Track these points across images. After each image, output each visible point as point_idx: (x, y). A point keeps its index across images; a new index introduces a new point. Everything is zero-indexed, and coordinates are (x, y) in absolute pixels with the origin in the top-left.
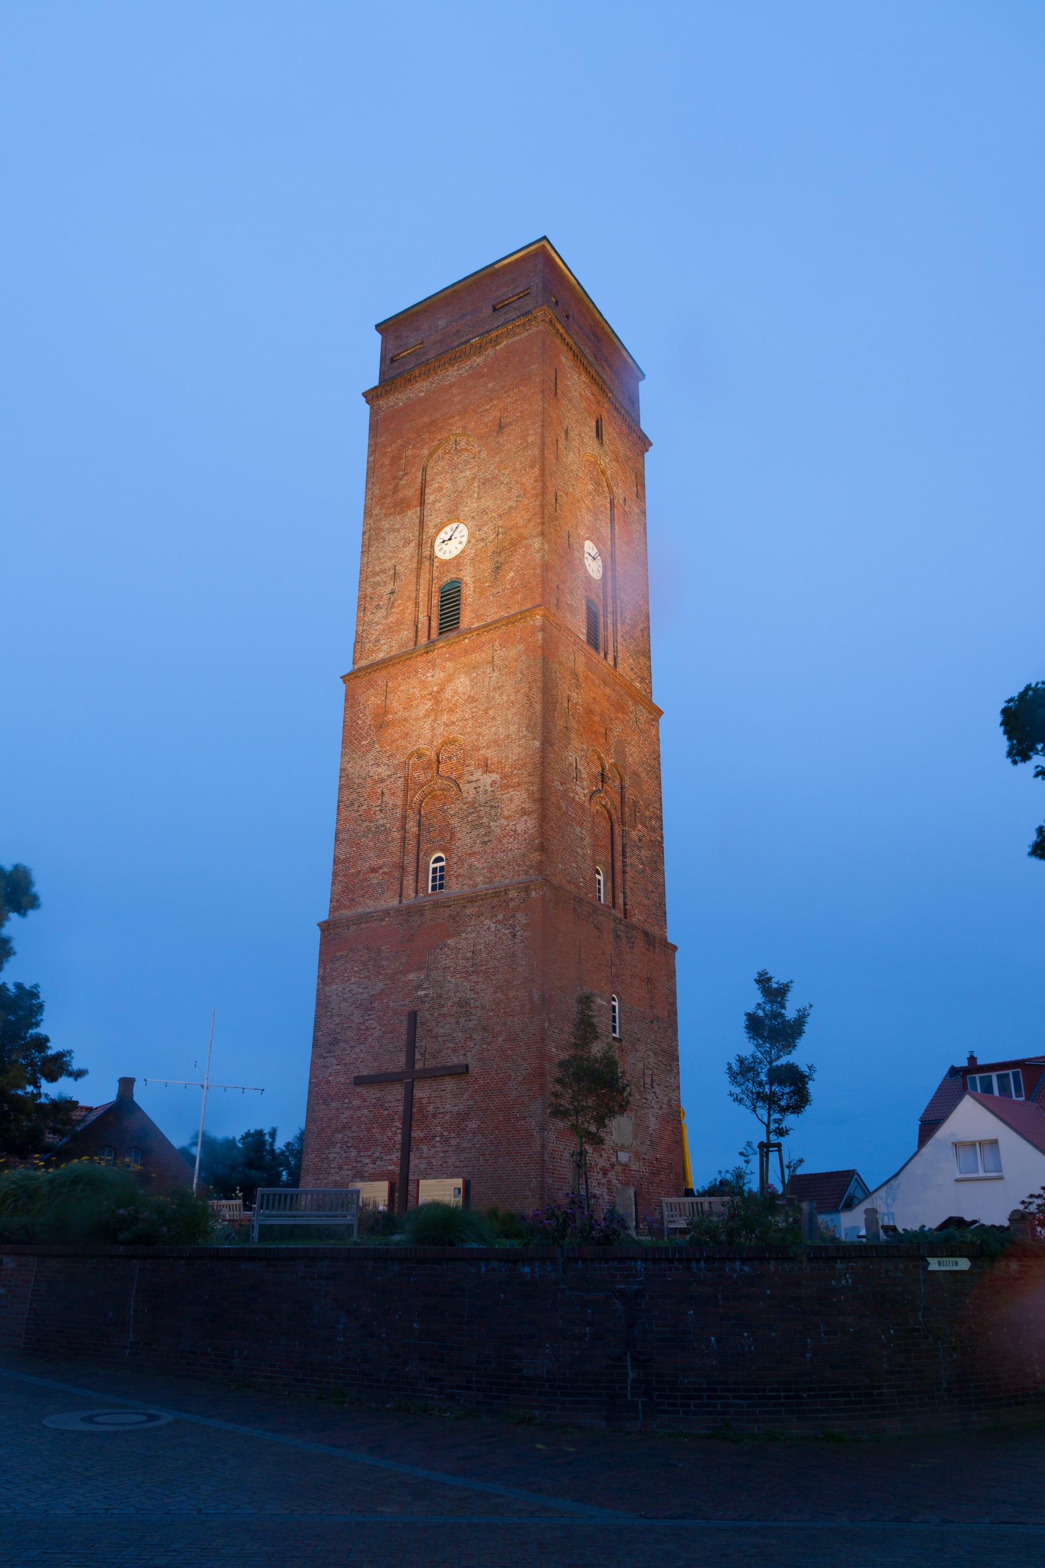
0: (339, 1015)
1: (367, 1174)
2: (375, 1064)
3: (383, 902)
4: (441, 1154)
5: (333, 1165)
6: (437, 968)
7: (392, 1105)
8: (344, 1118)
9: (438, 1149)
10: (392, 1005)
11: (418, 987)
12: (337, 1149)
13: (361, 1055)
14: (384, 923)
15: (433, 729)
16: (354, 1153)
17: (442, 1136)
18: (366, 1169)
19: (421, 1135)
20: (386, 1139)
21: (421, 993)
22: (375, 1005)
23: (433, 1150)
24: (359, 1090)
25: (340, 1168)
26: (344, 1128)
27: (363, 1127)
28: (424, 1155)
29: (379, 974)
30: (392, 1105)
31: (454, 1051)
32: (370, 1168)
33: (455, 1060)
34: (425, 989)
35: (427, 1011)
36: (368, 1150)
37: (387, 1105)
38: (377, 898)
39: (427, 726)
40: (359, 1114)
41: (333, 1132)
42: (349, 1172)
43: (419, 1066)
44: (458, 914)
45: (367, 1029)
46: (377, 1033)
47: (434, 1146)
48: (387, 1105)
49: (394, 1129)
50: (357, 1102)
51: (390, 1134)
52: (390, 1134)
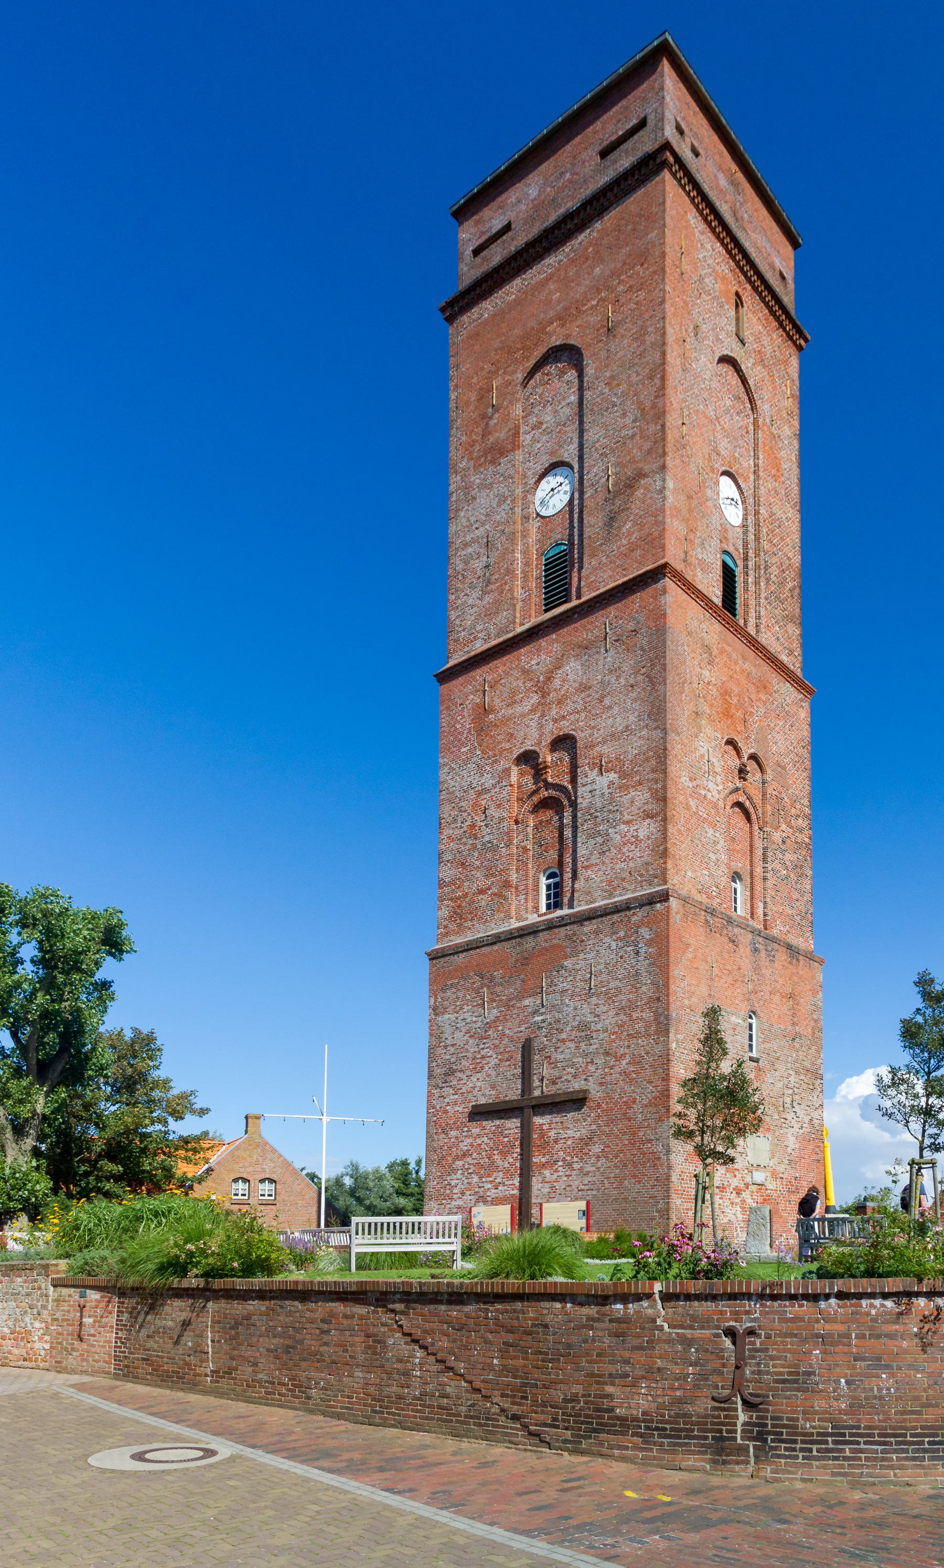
0: (453, 1045)
1: (489, 1199)
2: (493, 1092)
3: (493, 925)
4: (565, 1178)
5: (455, 1191)
6: (554, 992)
7: (512, 1132)
8: (464, 1146)
9: (560, 1174)
10: (507, 1032)
11: (535, 1012)
12: (459, 1175)
13: (479, 1084)
14: (496, 947)
15: (541, 726)
16: (475, 1179)
17: (564, 1160)
18: (488, 1194)
19: (543, 1160)
20: (507, 1165)
21: (538, 1018)
22: (490, 1032)
23: (556, 1175)
24: (477, 1118)
25: (463, 1194)
26: (464, 1155)
27: (484, 1154)
28: (547, 1180)
29: (492, 1000)
30: (512, 1132)
31: (575, 1077)
32: (492, 1193)
33: (576, 1085)
34: (542, 1014)
35: (546, 1037)
36: (489, 1176)
37: (506, 1132)
38: (486, 921)
39: (533, 724)
40: (479, 1141)
41: (454, 1160)
42: (472, 1197)
43: (537, 1093)
44: (574, 934)
45: (483, 1057)
46: (493, 1062)
47: (557, 1171)
48: (506, 1132)
49: (515, 1155)
50: (476, 1131)
51: (511, 1160)
52: (511, 1160)
